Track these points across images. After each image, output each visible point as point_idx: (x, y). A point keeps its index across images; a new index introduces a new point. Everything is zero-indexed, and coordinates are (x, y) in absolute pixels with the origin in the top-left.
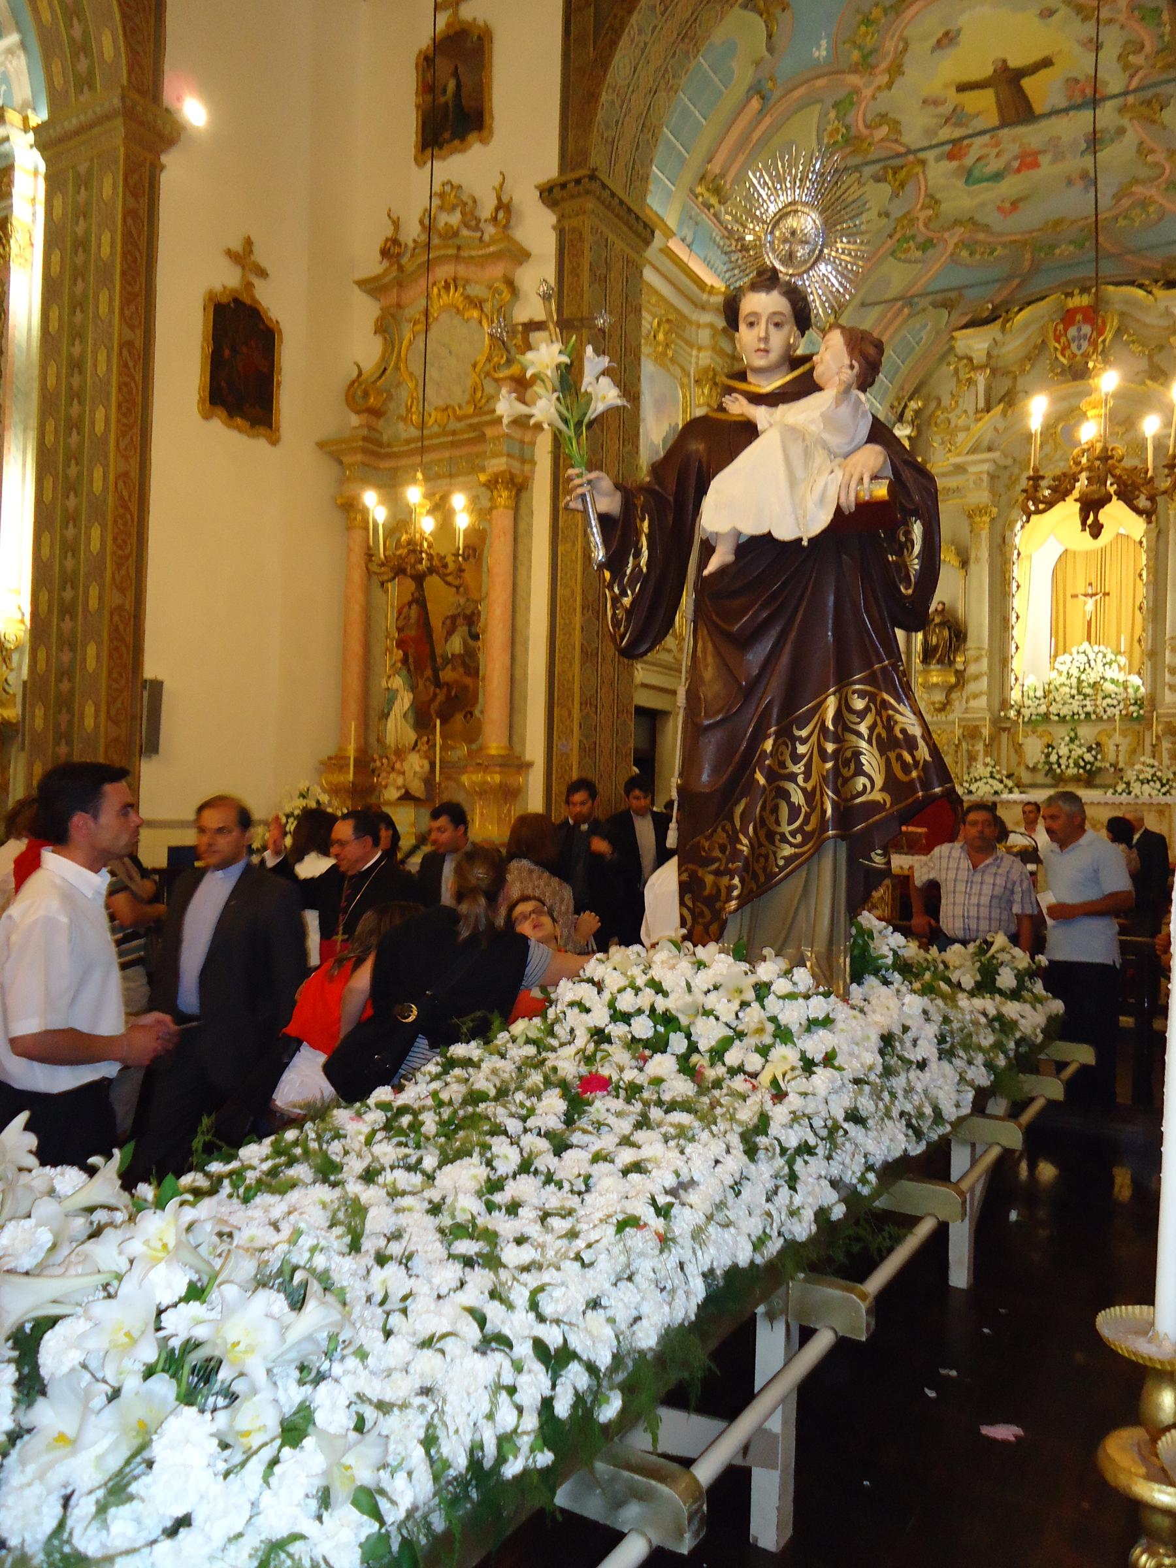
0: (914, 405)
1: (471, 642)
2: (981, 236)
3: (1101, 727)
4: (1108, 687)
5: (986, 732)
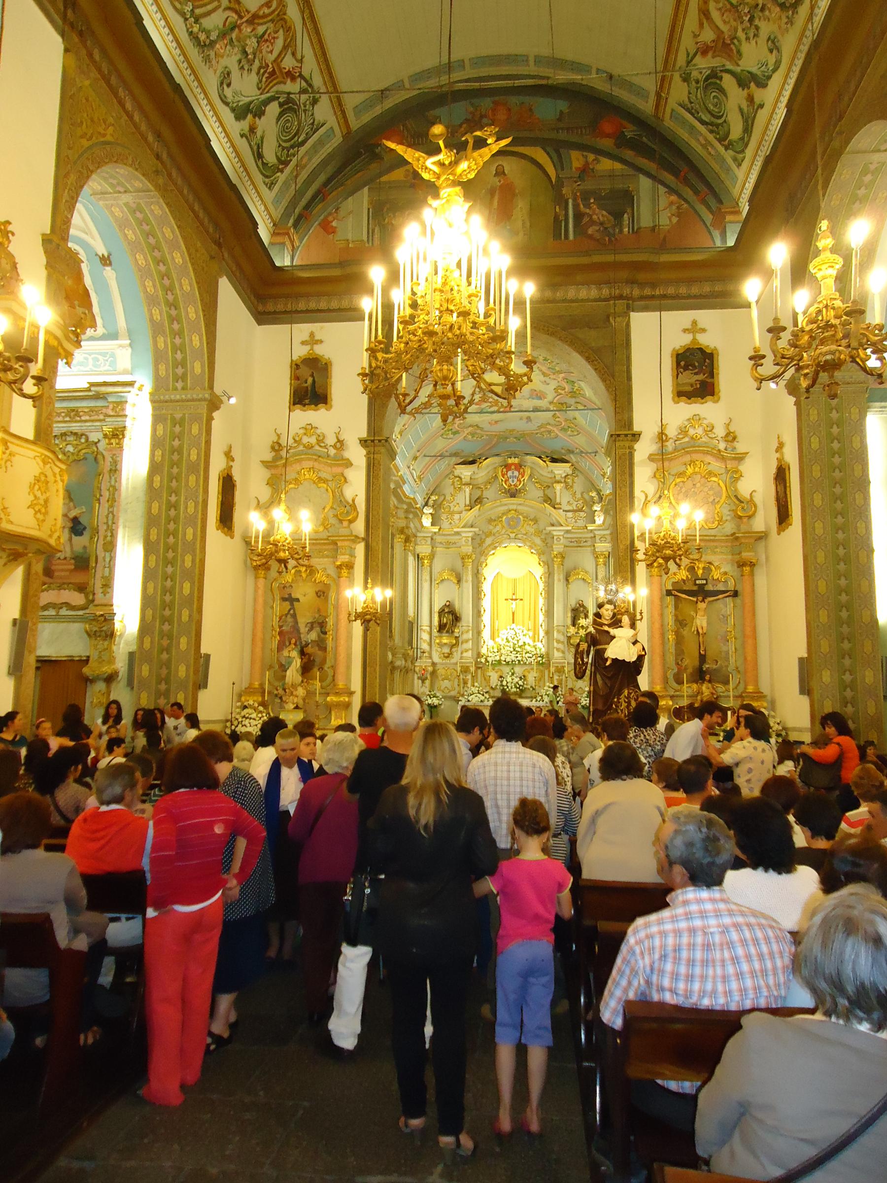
0: (433, 498)
1: (322, 636)
2: (478, 431)
3: (525, 667)
4: (528, 648)
5: (473, 669)
